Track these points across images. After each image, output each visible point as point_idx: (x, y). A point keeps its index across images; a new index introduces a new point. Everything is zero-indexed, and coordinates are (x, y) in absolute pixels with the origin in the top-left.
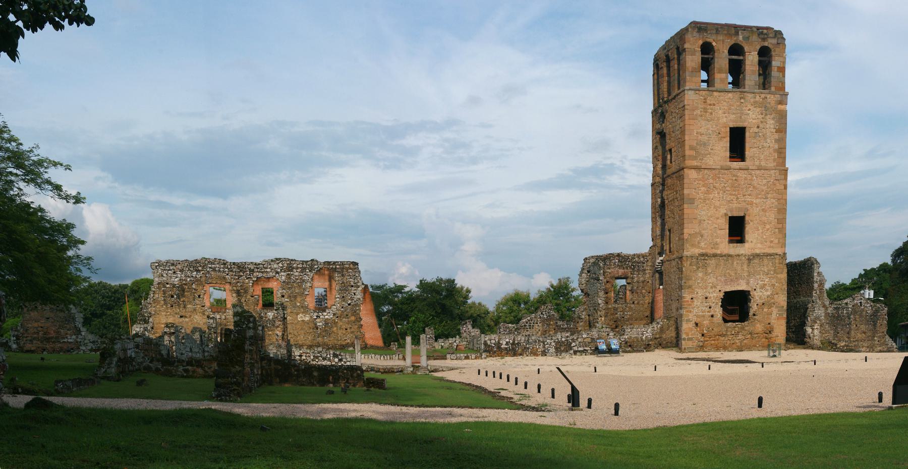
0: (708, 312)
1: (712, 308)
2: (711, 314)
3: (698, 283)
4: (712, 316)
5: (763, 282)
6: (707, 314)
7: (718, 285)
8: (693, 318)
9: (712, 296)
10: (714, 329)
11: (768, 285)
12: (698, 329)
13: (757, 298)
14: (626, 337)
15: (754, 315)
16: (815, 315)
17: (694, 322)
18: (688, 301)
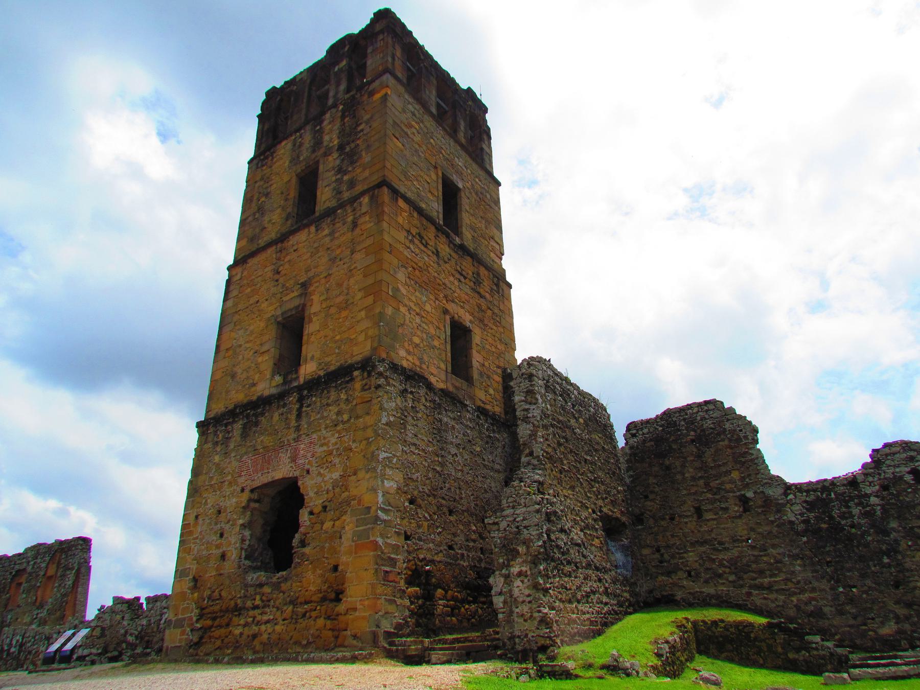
0: (218, 547)
1: (225, 535)
2: (221, 551)
3: (211, 478)
4: (223, 557)
5: (325, 448)
6: (214, 552)
7: (240, 476)
8: (191, 566)
9: (228, 503)
10: (224, 594)
11: (335, 452)
12: (196, 595)
13: (312, 494)
14: (144, 622)
15: (303, 544)
16: (503, 525)
17: (191, 577)
18: (189, 524)
